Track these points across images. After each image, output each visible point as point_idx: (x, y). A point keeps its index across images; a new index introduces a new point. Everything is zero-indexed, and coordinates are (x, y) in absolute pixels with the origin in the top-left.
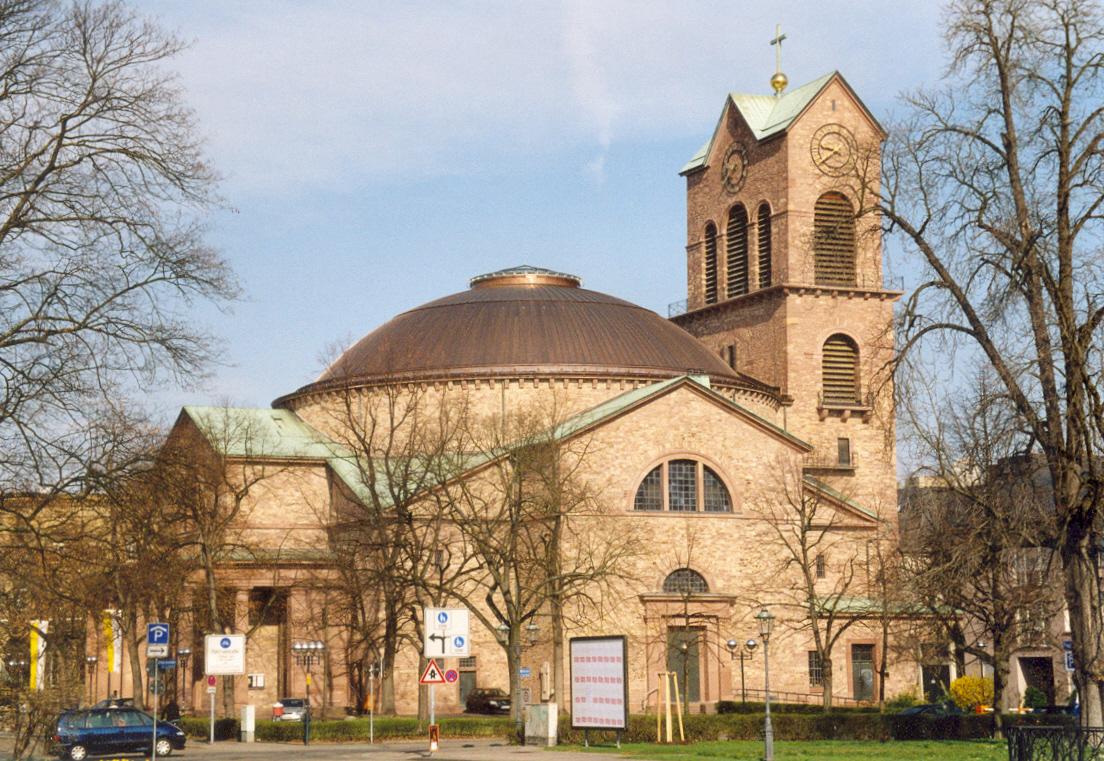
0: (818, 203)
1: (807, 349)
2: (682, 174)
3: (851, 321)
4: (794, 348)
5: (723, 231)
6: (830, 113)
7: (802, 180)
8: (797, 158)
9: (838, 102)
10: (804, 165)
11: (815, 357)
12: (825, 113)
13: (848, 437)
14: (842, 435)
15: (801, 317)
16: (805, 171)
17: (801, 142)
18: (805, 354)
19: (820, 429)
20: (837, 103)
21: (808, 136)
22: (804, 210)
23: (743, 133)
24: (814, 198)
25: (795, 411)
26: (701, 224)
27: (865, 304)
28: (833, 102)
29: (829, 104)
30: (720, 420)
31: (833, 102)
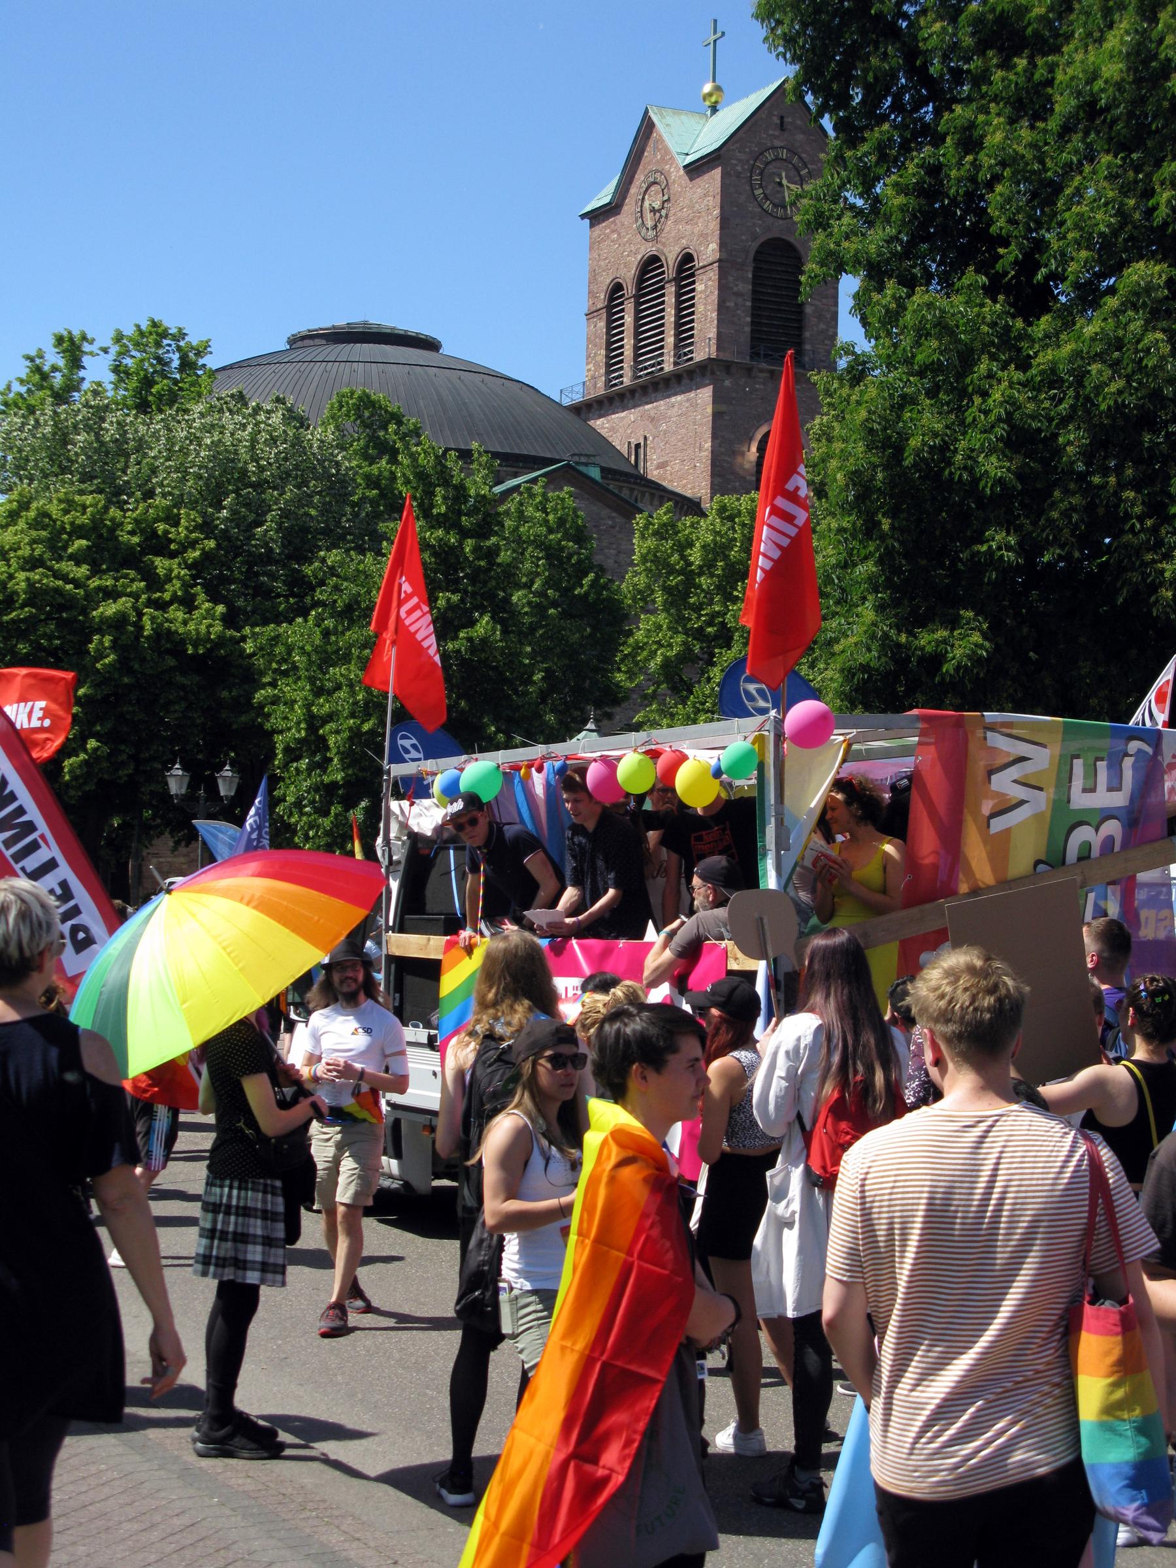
0: (757, 252)
2: (583, 216)
5: (630, 289)
6: (777, 133)
9: (788, 120)
12: (771, 132)
17: (739, 168)
20: (786, 120)
21: (748, 161)
23: (663, 158)
24: (754, 246)
26: (605, 281)
28: (782, 118)
29: (777, 121)
30: (613, 527)
31: (782, 118)
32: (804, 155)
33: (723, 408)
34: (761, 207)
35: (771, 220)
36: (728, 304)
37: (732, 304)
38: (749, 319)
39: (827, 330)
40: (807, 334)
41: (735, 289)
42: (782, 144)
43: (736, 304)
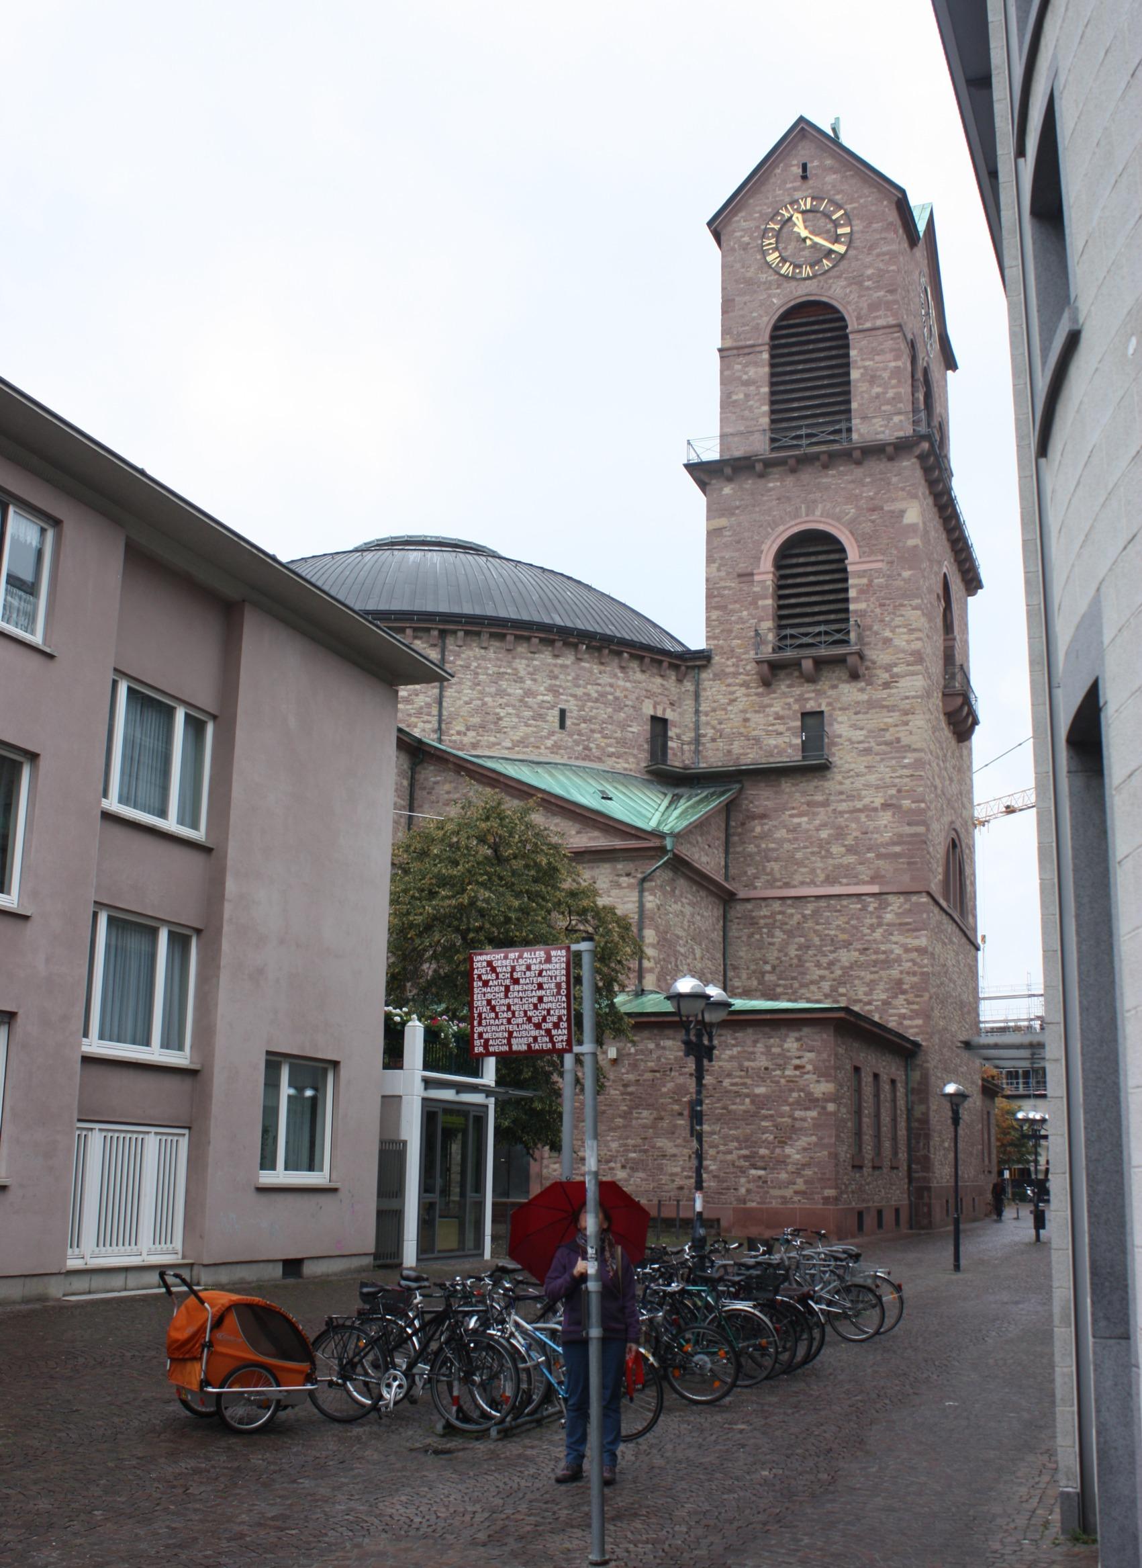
1: (742, 567)
3: (829, 505)
4: (719, 570)
7: (747, 298)
8: (738, 266)
10: (749, 275)
11: (757, 578)
12: (789, 186)
13: (823, 708)
14: (811, 706)
15: (733, 514)
16: (750, 282)
17: (746, 239)
18: (740, 576)
19: (766, 700)
20: (809, 165)
21: (758, 227)
22: (751, 342)
24: (766, 322)
25: (717, 677)
27: (858, 472)
32: (838, 197)
33: (723, 522)
34: (778, 273)
35: (794, 284)
36: (734, 397)
37: (741, 396)
38: (766, 408)
39: (887, 393)
40: (854, 405)
41: (745, 377)
42: (806, 194)
43: (747, 396)
